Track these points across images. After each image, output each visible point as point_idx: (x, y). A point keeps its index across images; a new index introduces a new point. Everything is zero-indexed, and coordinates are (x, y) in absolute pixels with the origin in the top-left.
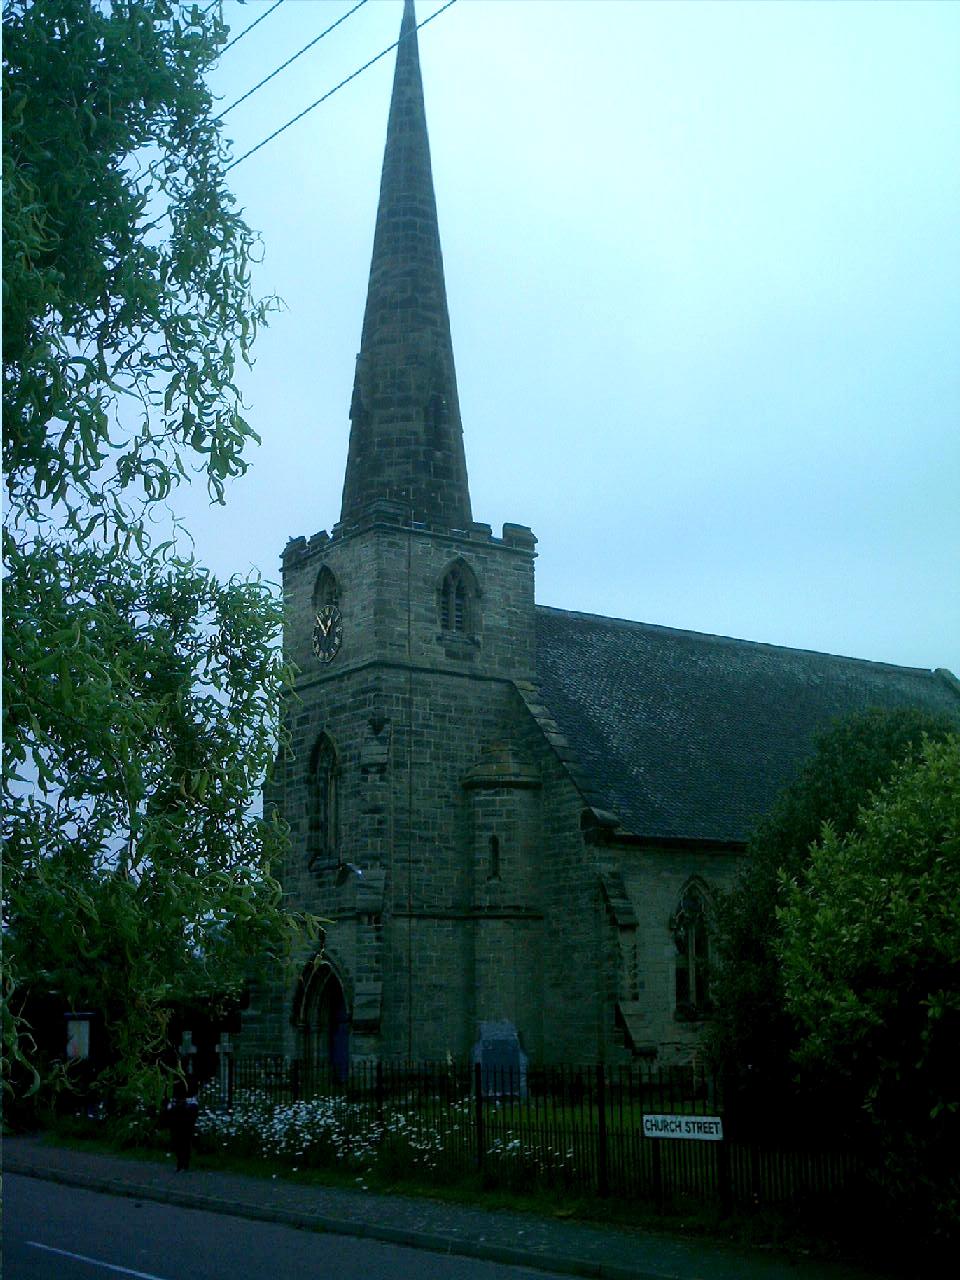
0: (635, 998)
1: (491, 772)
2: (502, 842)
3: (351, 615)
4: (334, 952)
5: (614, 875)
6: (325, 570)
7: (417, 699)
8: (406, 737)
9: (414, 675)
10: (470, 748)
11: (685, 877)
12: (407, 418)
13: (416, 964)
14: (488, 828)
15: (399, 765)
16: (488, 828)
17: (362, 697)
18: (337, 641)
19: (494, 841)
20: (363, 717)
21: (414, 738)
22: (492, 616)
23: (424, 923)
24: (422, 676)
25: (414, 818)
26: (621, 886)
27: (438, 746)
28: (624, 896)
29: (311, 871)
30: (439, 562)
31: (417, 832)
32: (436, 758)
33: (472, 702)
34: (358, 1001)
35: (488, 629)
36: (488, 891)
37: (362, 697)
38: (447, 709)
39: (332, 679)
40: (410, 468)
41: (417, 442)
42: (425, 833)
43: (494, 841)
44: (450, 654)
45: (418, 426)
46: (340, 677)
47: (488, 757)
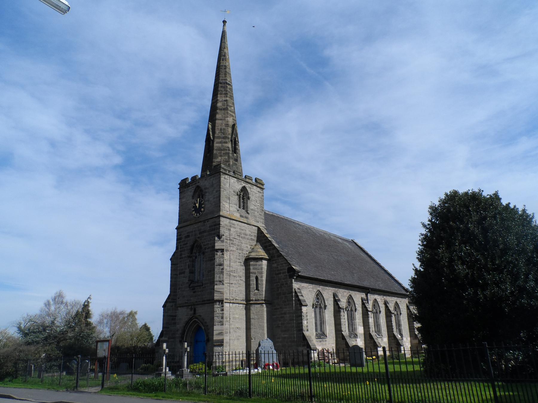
0: (308, 330)
1: (253, 255)
2: (259, 278)
3: (208, 201)
4: (200, 316)
5: (299, 289)
6: (198, 187)
7: (232, 229)
8: (229, 241)
9: (231, 221)
10: (247, 247)
11: (315, 290)
12: (226, 143)
13: (231, 320)
14: (255, 273)
15: (227, 250)
16: (255, 273)
17: (213, 227)
18: (202, 210)
19: (257, 278)
20: (214, 234)
21: (231, 242)
22: (252, 205)
23: (234, 305)
24: (234, 222)
25: (231, 269)
26: (300, 292)
27: (238, 245)
28: (302, 296)
29: (190, 288)
30: (238, 186)
31: (232, 274)
32: (237, 249)
33: (248, 232)
34: (215, 332)
35: (252, 210)
36: (255, 294)
37: (213, 227)
38: (240, 233)
39: (201, 222)
40: (227, 157)
41: (229, 150)
42: (235, 274)
43: (257, 278)
44: (241, 216)
45: (229, 145)
46: (204, 221)
47: (253, 250)
